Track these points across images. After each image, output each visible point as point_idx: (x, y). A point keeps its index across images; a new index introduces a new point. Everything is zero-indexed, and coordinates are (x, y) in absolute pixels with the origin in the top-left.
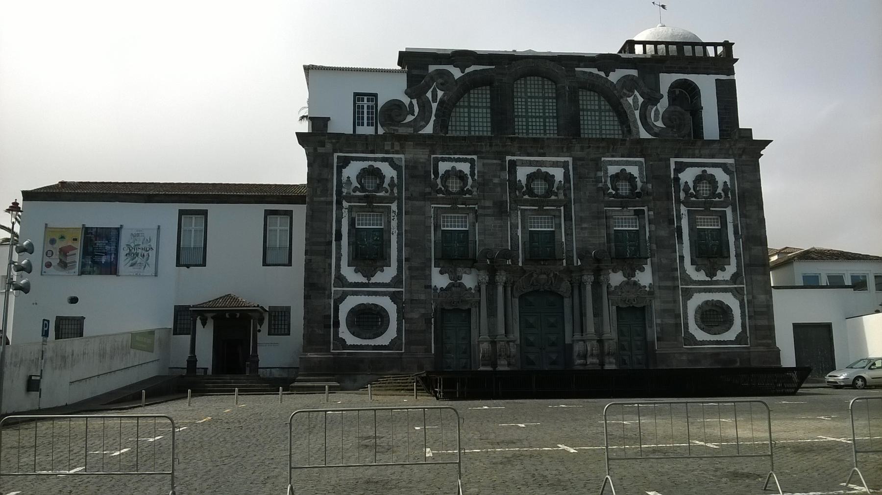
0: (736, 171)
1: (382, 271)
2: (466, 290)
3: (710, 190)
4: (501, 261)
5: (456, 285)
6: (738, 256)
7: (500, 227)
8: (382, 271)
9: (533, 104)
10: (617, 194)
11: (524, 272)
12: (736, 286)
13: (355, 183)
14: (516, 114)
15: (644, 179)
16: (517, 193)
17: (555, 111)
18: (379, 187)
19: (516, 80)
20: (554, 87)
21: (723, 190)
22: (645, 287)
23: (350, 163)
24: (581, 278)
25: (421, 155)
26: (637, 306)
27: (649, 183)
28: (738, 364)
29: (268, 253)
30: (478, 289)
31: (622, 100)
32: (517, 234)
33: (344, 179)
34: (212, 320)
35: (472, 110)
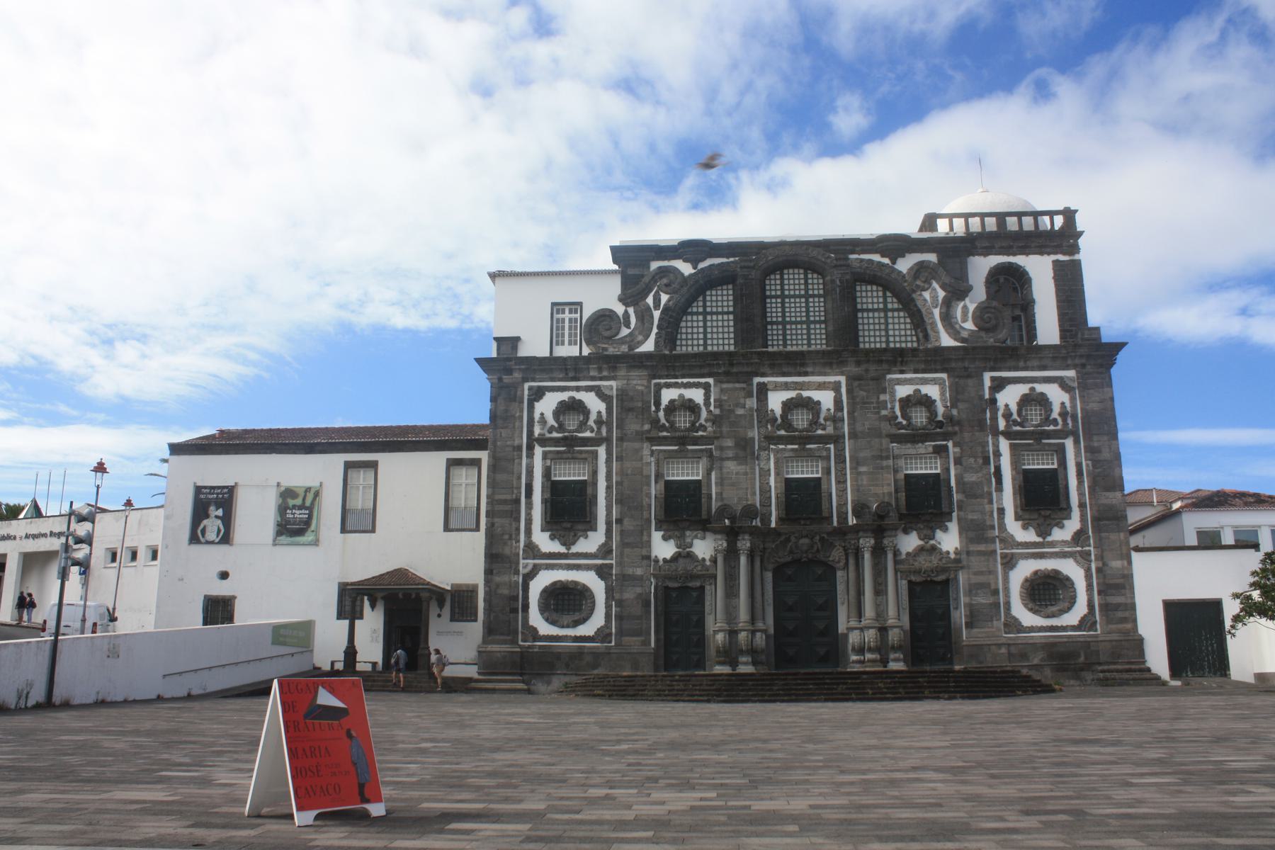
0: (1078, 388)
1: (586, 537)
3: (1041, 415)
5: (685, 555)
6: (1082, 505)
7: (746, 474)
8: (586, 537)
9: (793, 305)
11: (779, 534)
12: (1079, 549)
13: (551, 421)
14: (769, 319)
16: (769, 427)
17: (822, 314)
18: (583, 425)
19: (769, 275)
20: (821, 281)
21: (1060, 414)
22: (948, 553)
23: (544, 394)
25: (638, 381)
26: (935, 579)
28: (1082, 659)
29: (452, 515)
30: (714, 560)
31: (914, 296)
32: (768, 483)
33: (537, 416)
34: (383, 602)
35: (709, 318)
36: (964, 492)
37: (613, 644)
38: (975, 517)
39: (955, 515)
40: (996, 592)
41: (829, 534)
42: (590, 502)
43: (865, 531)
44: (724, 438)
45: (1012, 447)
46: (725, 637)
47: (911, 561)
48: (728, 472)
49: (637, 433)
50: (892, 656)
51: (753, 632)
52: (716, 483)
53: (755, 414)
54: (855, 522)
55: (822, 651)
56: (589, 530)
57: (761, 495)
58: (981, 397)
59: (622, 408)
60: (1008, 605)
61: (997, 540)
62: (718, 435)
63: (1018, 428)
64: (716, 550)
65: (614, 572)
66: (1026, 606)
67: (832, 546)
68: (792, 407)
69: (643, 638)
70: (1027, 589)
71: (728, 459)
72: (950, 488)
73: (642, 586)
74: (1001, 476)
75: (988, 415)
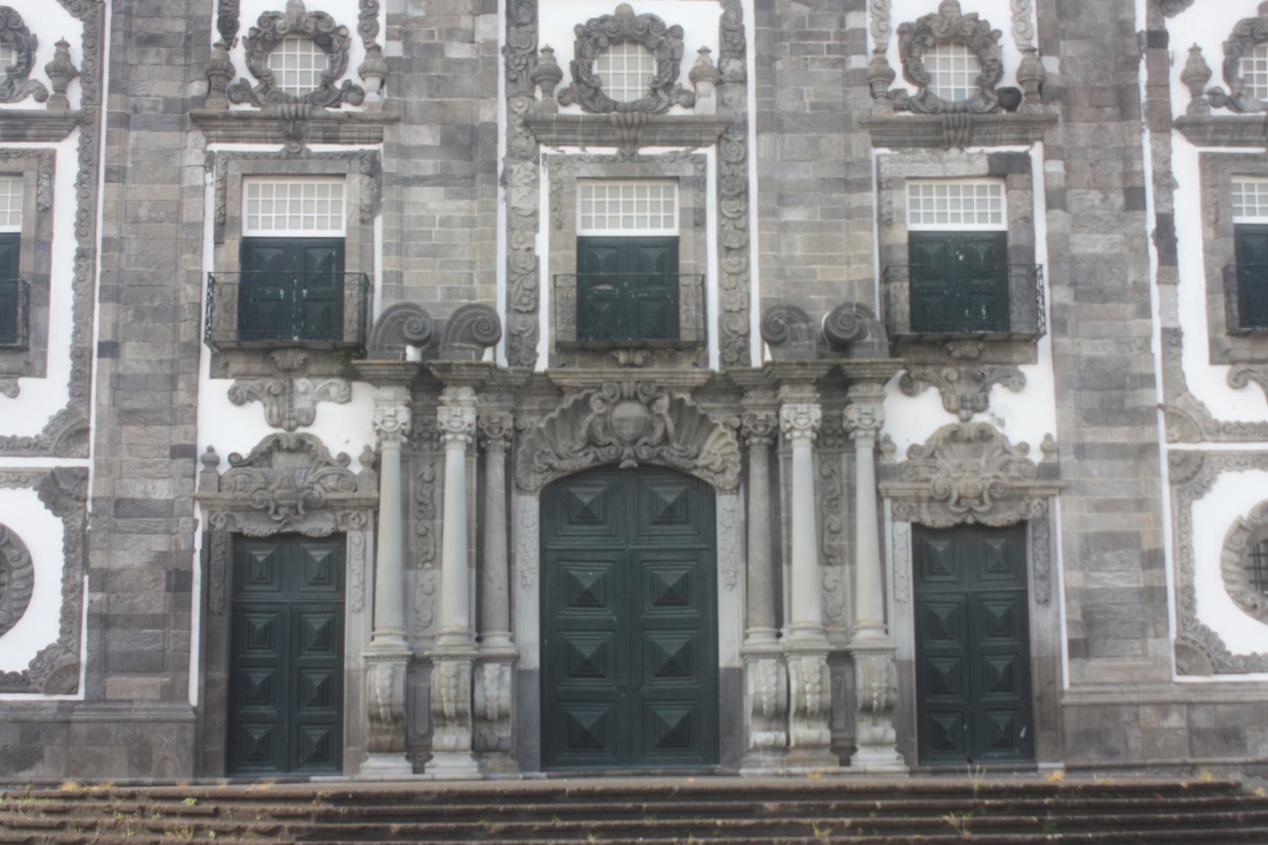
2: (328, 464)
4: (460, 348)
7: (470, 222)
10: (925, 97)
11: (560, 391)
15: (1030, 39)
16: (539, 94)
22: (1024, 448)
24: (778, 416)
26: (989, 521)
27: (1049, 54)
30: (375, 464)
36: (1073, 284)
37: (81, 696)
38: (1102, 354)
39: (1044, 343)
40: (1154, 559)
41: (696, 391)
42: (27, 294)
43: (794, 382)
44: (410, 122)
45: (1207, 162)
46: (393, 677)
47: (924, 473)
48: (420, 219)
49: (169, 104)
50: (866, 730)
51: (478, 663)
52: (385, 246)
53: (501, 60)
54: (768, 357)
55: (672, 716)
56: (22, 375)
57: (509, 282)
58: (1125, 27)
59: (128, 35)
60: (1187, 595)
61: (1161, 416)
62: (394, 114)
63: (1224, 112)
64: (379, 432)
65: (90, 492)
66: (1238, 599)
67: (705, 425)
68: (603, 41)
69: (167, 679)
70: (1240, 553)
71: (421, 180)
72: (1033, 272)
73: (168, 532)
74: (1175, 240)
75: (1143, 75)
